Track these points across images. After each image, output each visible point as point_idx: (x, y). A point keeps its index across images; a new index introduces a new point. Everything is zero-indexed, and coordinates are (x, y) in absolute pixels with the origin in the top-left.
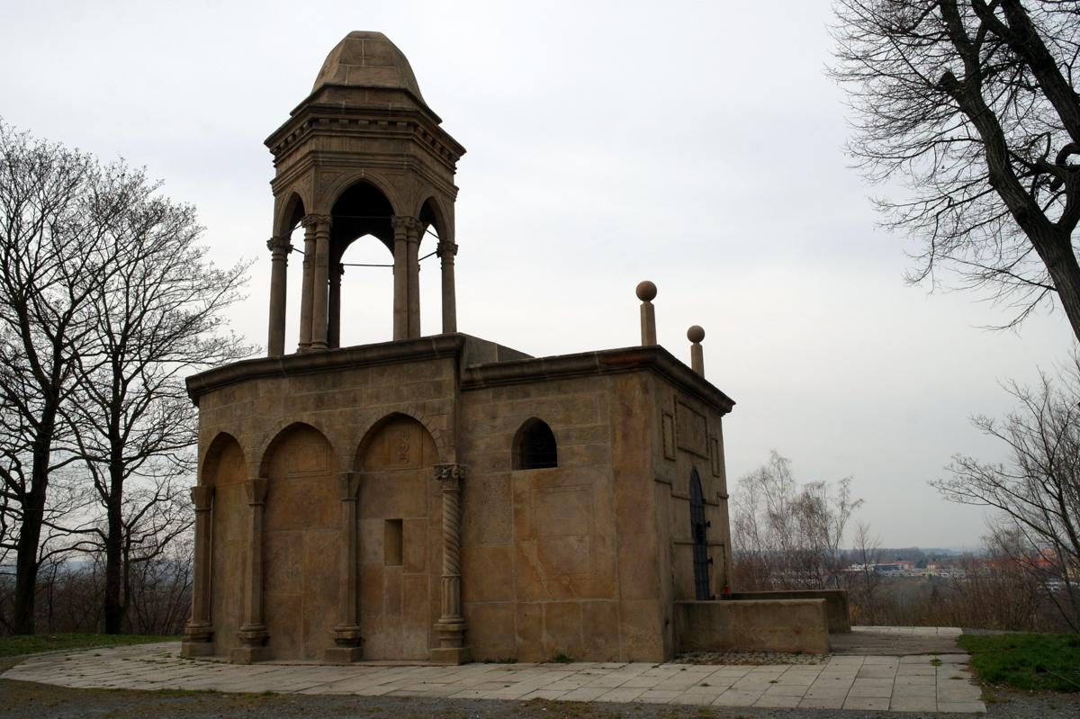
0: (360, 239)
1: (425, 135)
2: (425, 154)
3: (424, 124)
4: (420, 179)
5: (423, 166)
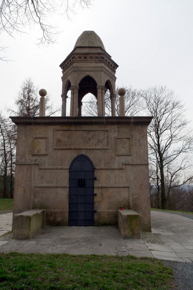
0: (86, 95)
1: (80, 57)
2: (82, 63)
3: (77, 55)
4: (79, 72)
5: (79, 68)
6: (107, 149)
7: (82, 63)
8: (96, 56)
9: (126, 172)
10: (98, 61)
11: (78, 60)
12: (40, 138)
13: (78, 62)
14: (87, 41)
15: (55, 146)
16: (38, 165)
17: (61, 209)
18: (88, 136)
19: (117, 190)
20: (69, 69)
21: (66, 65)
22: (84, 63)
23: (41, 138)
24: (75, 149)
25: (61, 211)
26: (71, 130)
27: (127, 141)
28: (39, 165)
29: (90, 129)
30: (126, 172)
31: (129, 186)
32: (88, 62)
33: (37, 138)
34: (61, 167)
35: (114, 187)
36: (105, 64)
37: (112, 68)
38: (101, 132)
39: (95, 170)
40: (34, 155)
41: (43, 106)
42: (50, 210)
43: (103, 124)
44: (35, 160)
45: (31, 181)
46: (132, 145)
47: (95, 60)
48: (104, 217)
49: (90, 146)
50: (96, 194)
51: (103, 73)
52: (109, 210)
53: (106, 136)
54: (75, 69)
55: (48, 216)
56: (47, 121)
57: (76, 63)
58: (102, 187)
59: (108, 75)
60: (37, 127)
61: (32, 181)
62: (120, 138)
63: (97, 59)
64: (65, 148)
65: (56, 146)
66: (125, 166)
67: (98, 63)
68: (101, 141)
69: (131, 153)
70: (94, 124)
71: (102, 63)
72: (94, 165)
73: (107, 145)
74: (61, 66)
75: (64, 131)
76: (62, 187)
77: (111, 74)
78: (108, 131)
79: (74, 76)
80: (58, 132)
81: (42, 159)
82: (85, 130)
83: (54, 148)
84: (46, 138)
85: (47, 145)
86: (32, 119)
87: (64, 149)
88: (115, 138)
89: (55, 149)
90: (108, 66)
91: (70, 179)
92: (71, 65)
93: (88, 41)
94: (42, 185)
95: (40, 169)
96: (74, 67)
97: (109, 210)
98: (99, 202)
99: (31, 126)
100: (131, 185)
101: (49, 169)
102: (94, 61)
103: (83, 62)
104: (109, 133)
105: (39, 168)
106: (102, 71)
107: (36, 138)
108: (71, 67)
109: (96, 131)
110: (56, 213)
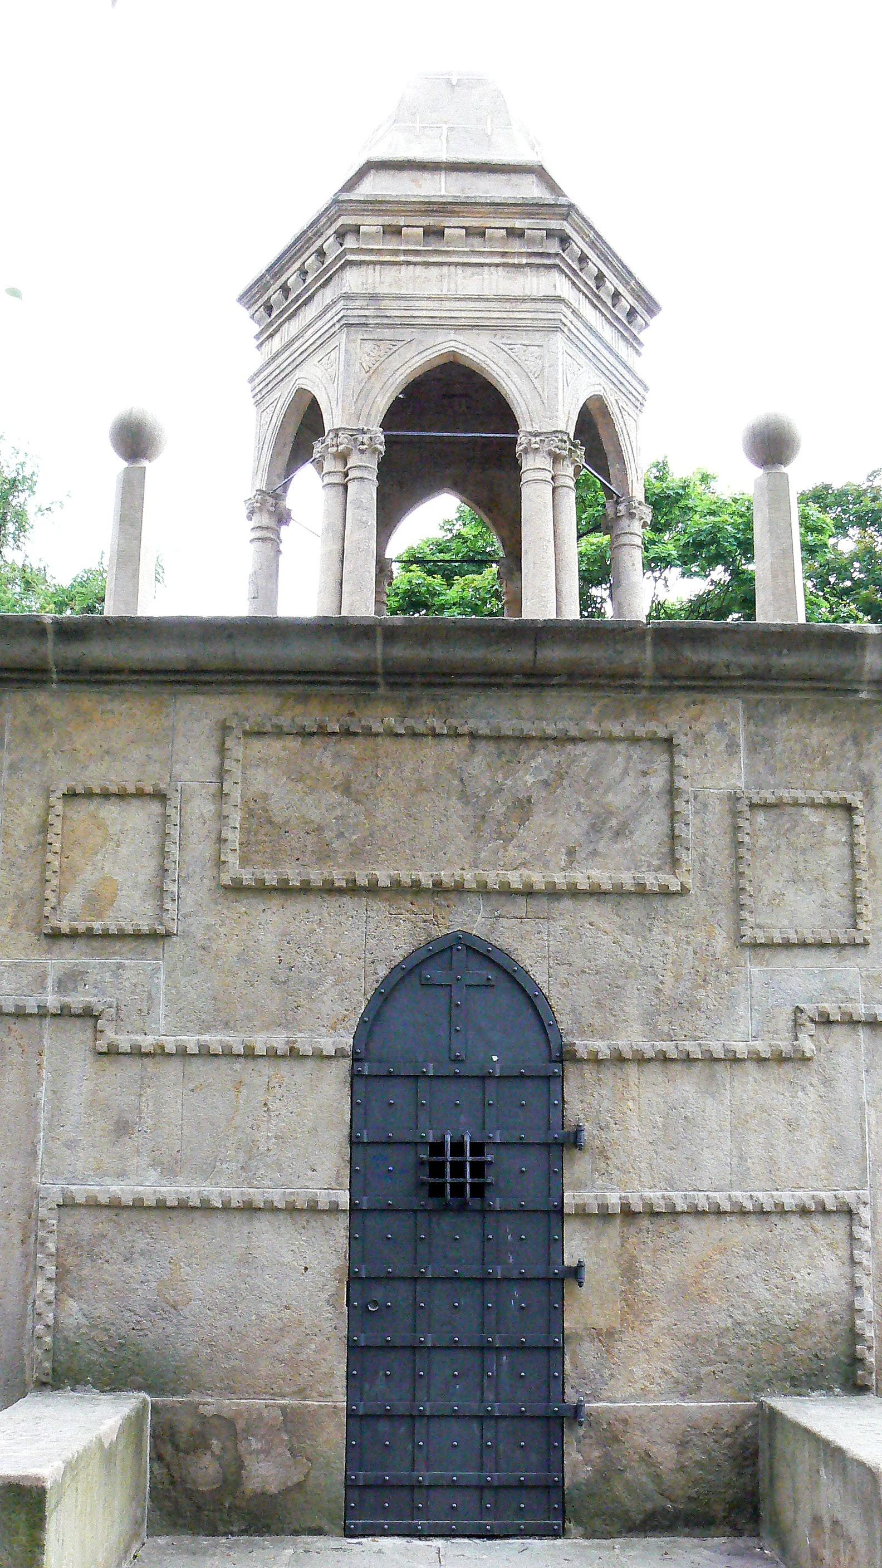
1: (396, 231)
2: (406, 272)
4: (388, 333)
5: (384, 304)
6: (666, 893)
7: (411, 267)
8: (509, 223)
9: (827, 1082)
10: (524, 261)
11: (379, 251)
12: (106, 795)
13: (382, 263)
14: (445, 127)
15: (233, 859)
16: (90, 1022)
17: (283, 1396)
18: (509, 782)
19: (754, 1230)
20: (310, 312)
21: (285, 290)
22: (419, 269)
23: (122, 796)
24: (397, 889)
25: (283, 1408)
26: (369, 733)
27: (834, 829)
28: (97, 1018)
29: (529, 728)
30: (827, 1082)
31: (849, 1196)
32: (456, 264)
33: (89, 795)
34: (279, 1041)
35: (732, 1213)
36: (574, 283)
37: (617, 319)
38: (621, 747)
39: (571, 1070)
40: (55, 936)
41: (138, 538)
42: (196, 1398)
43: (630, 687)
44: (68, 981)
45: (34, 1154)
46: (871, 859)
47: (504, 254)
48: (646, 1457)
49: (524, 864)
50: (580, 1266)
51: (559, 341)
52: (690, 1405)
53: (657, 782)
54: (355, 312)
55: (176, 1448)
56: (174, 654)
57: (363, 268)
58: (628, 1213)
59: (593, 357)
60: (87, 700)
61: (41, 1148)
62: (772, 799)
63: (516, 246)
64: (316, 876)
65: (245, 861)
66: (821, 1033)
67: (527, 270)
68: (614, 822)
69: (861, 925)
70: (560, 685)
71: (555, 276)
72: (564, 1021)
73: (674, 862)
74: (249, 297)
75: (312, 734)
76: (292, 1209)
77: (617, 356)
78: (675, 742)
79: (348, 364)
80: (258, 747)
81: (120, 966)
82: (484, 730)
83: (226, 879)
84: (160, 797)
85: (163, 854)
86: (50, 637)
87: (306, 889)
88: (734, 798)
89: (237, 889)
90: (595, 301)
91: (354, 1142)
92: (324, 285)
93: (451, 129)
94: (122, 1190)
95: (112, 1052)
96: (348, 297)
97: (690, 1405)
98: (607, 1337)
99: (41, 698)
100: (866, 1194)
101: (183, 1053)
102: (497, 260)
103: (414, 264)
104: (680, 760)
105: (102, 1045)
106: (556, 328)
107: (80, 790)
108: (327, 295)
109: (573, 740)
110: (240, 1424)
